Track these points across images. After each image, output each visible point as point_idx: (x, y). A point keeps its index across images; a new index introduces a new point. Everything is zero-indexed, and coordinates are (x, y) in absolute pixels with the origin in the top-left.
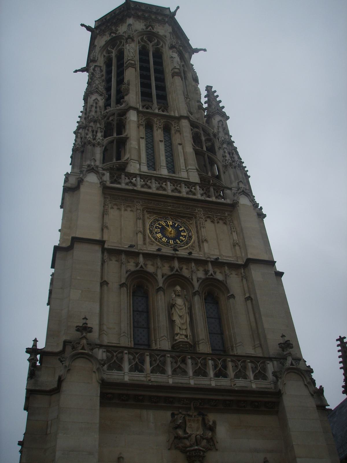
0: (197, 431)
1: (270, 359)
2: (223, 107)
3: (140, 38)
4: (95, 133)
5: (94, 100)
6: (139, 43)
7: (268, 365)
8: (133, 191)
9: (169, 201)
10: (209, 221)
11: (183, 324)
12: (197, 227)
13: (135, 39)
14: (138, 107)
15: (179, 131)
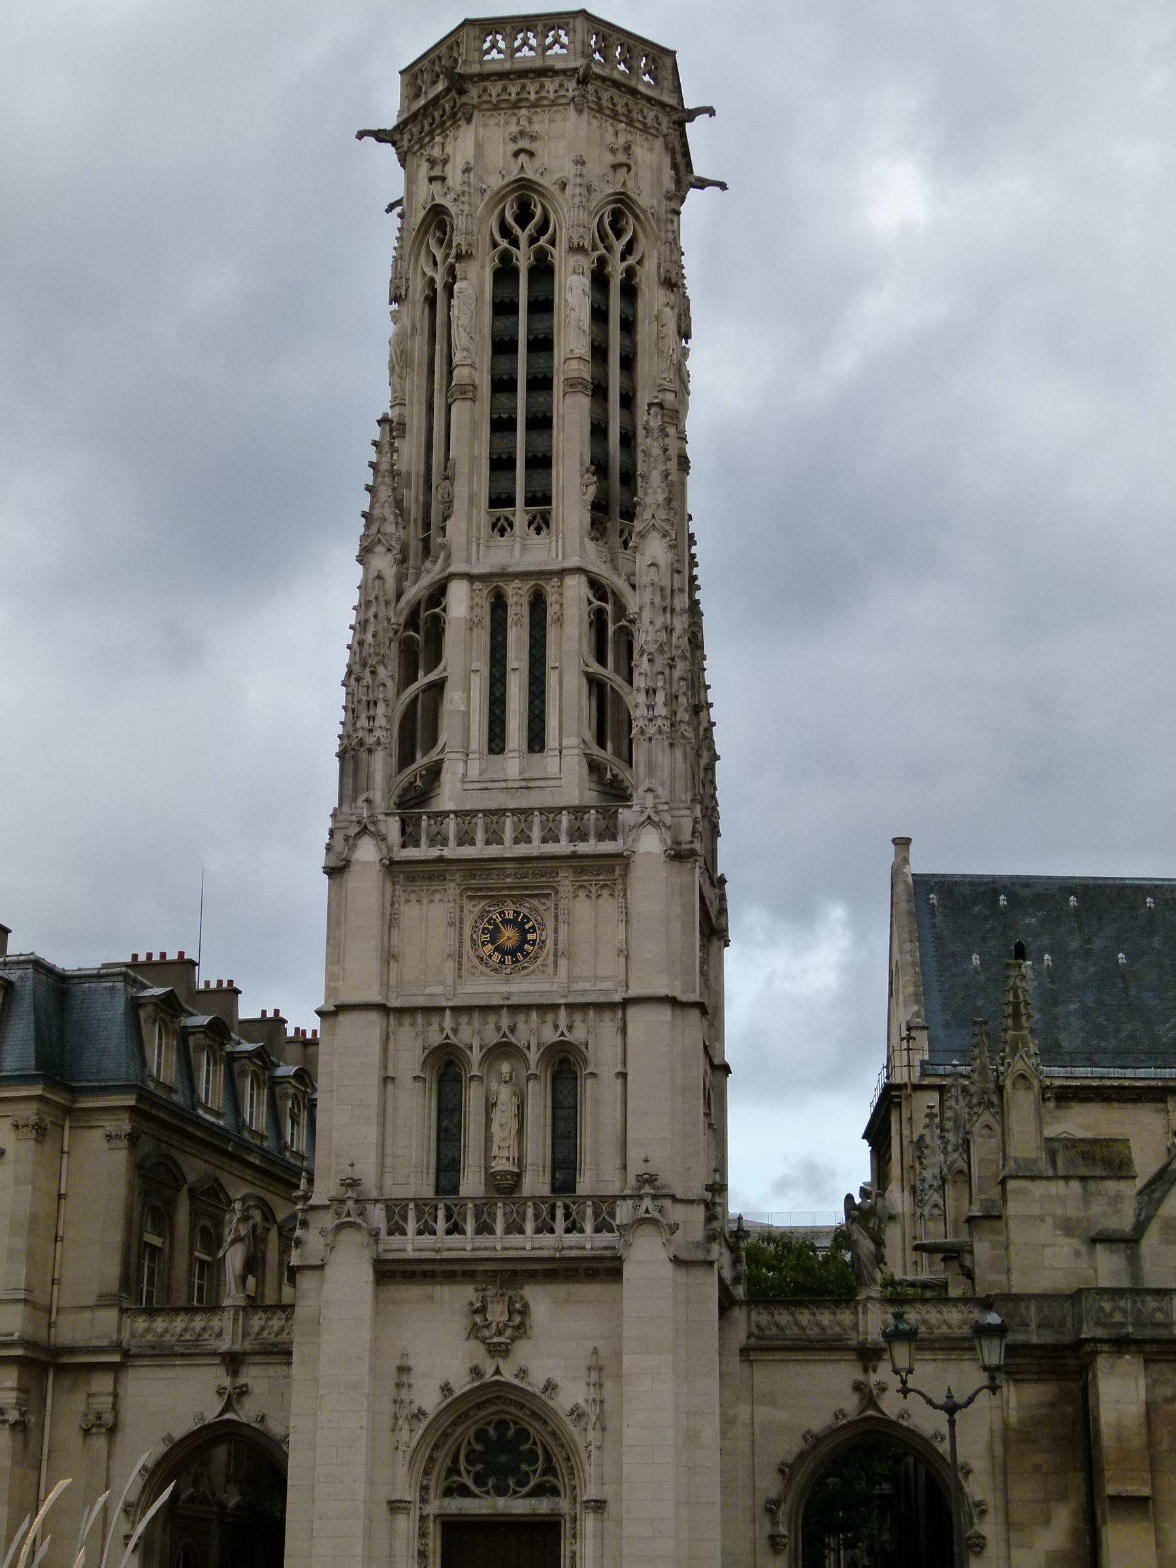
0: (501, 1315)
1: (624, 1198)
6: (495, 245)
7: (618, 1209)
8: (441, 860)
9: (507, 866)
10: (582, 894)
11: (504, 1139)
12: (556, 917)
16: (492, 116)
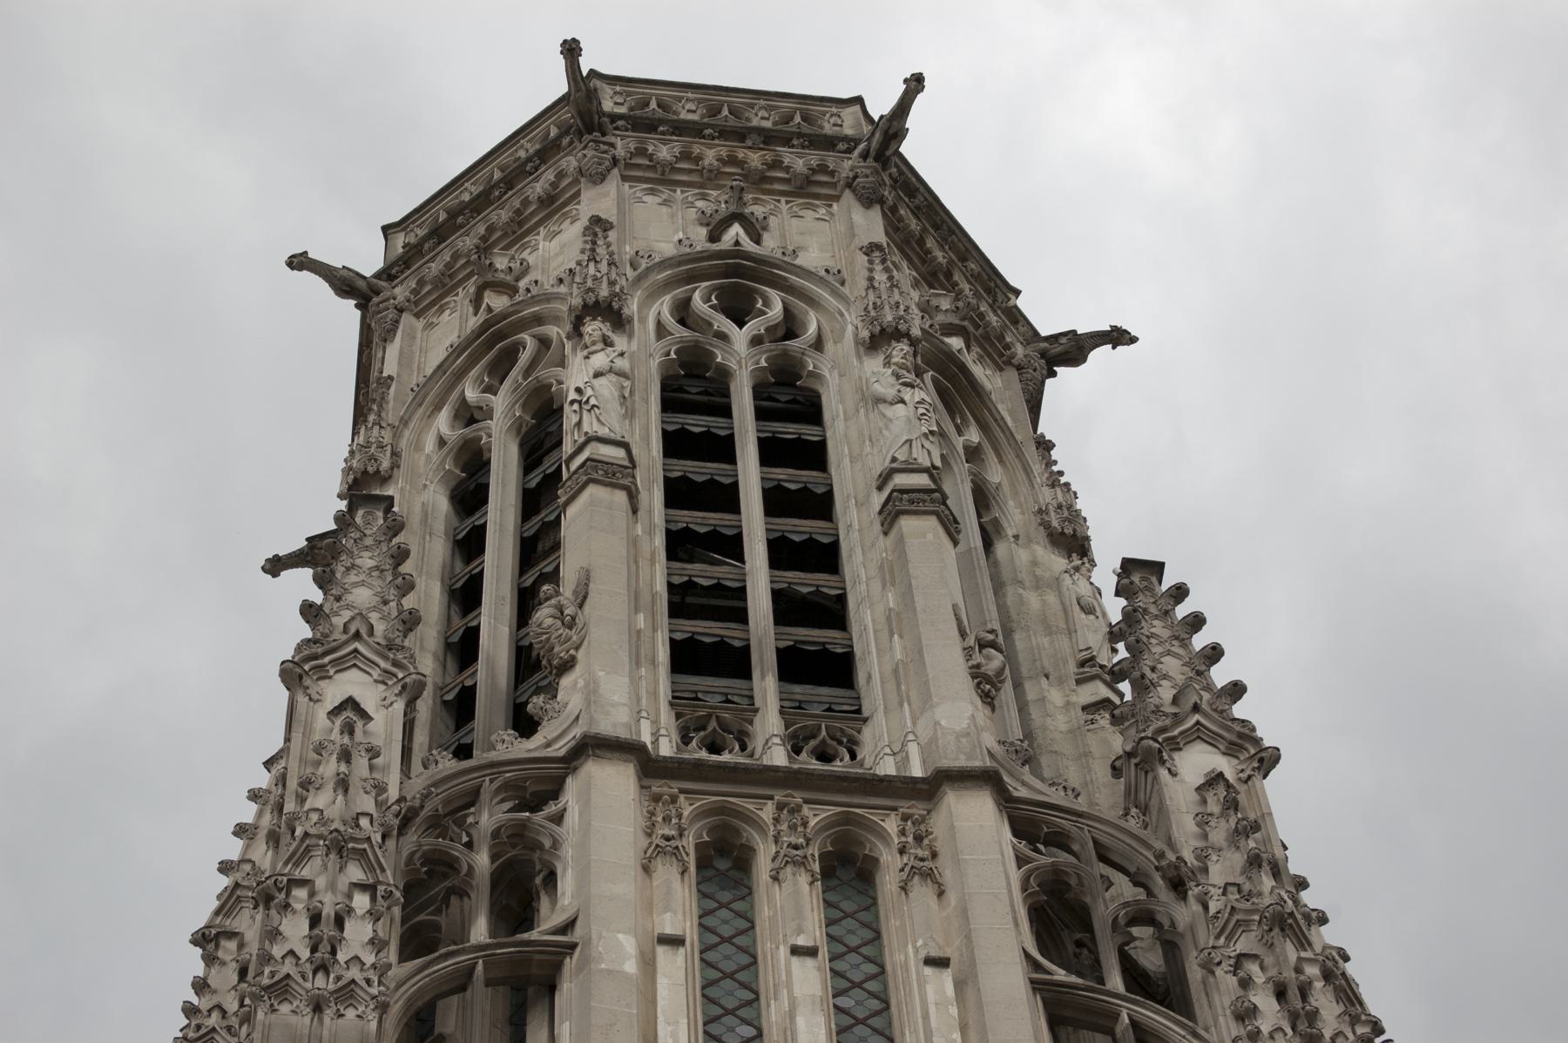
2: (1236, 690)
3: (663, 307)
4: (327, 930)
5: (335, 712)
13: (632, 307)
14: (646, 738)
15: (929, 875)
16: (652, 192)
